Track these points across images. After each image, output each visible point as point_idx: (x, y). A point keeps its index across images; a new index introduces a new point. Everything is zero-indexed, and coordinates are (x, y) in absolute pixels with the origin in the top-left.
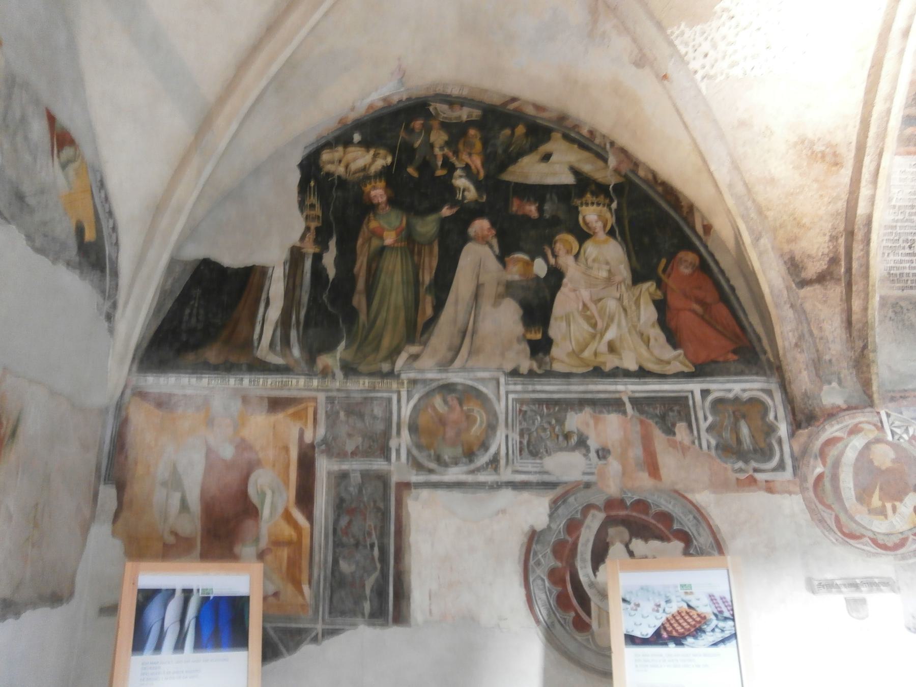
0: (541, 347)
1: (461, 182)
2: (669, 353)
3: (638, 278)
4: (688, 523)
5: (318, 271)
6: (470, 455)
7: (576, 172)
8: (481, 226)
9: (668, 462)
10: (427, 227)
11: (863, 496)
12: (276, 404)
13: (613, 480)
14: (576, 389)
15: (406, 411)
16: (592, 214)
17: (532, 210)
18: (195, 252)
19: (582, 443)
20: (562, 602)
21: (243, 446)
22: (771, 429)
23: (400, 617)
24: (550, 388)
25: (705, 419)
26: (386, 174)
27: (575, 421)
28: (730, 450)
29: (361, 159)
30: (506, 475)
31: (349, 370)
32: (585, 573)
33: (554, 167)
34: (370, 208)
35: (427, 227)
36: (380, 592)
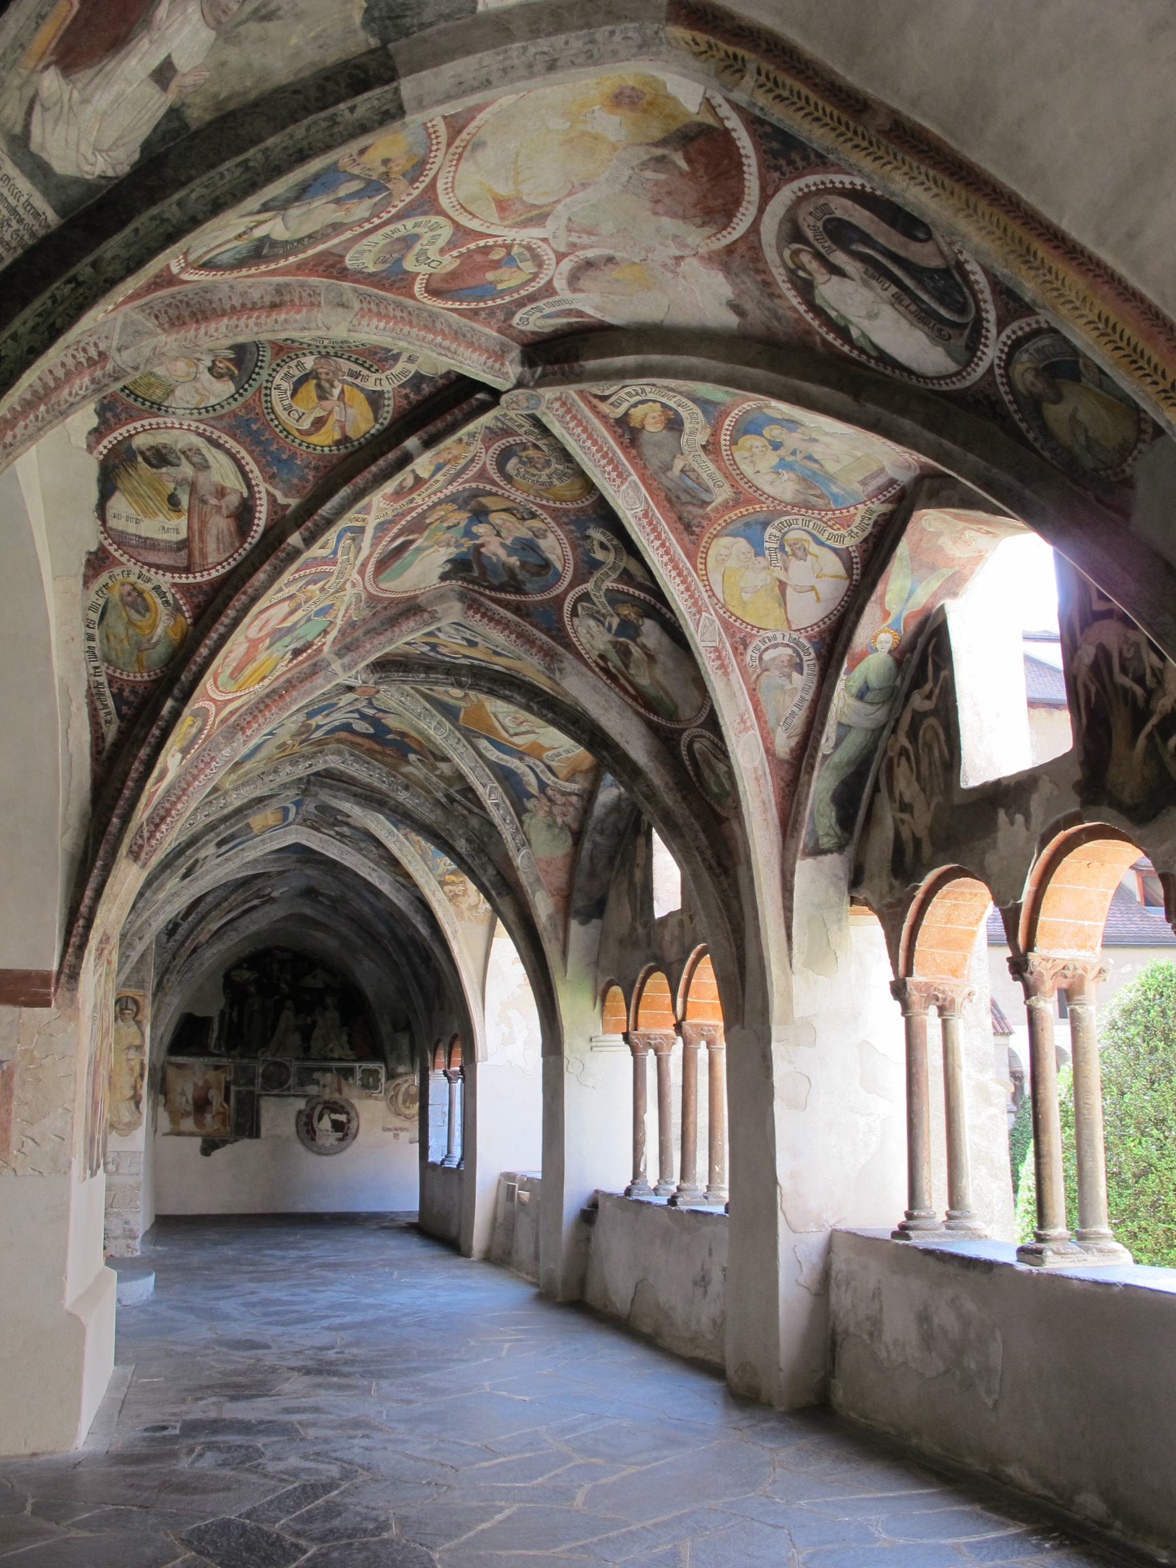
0: (307, 1049)
1: (283, 986)
8: (289, 1003)
9: (345, 1089)
11: (404, 1102)
12: (217, 1068)
13: (327, 1095)
16: (329, 1000)
18: (188, 1010)
21: (206, 1082)
23: (258, 1136)
24: (308, 1064)
25: (358, 1075)
27: (316, 1075)
28: (366, 1086)
29: (246, 975)
31: (242, 1056)
33: (317, 981)
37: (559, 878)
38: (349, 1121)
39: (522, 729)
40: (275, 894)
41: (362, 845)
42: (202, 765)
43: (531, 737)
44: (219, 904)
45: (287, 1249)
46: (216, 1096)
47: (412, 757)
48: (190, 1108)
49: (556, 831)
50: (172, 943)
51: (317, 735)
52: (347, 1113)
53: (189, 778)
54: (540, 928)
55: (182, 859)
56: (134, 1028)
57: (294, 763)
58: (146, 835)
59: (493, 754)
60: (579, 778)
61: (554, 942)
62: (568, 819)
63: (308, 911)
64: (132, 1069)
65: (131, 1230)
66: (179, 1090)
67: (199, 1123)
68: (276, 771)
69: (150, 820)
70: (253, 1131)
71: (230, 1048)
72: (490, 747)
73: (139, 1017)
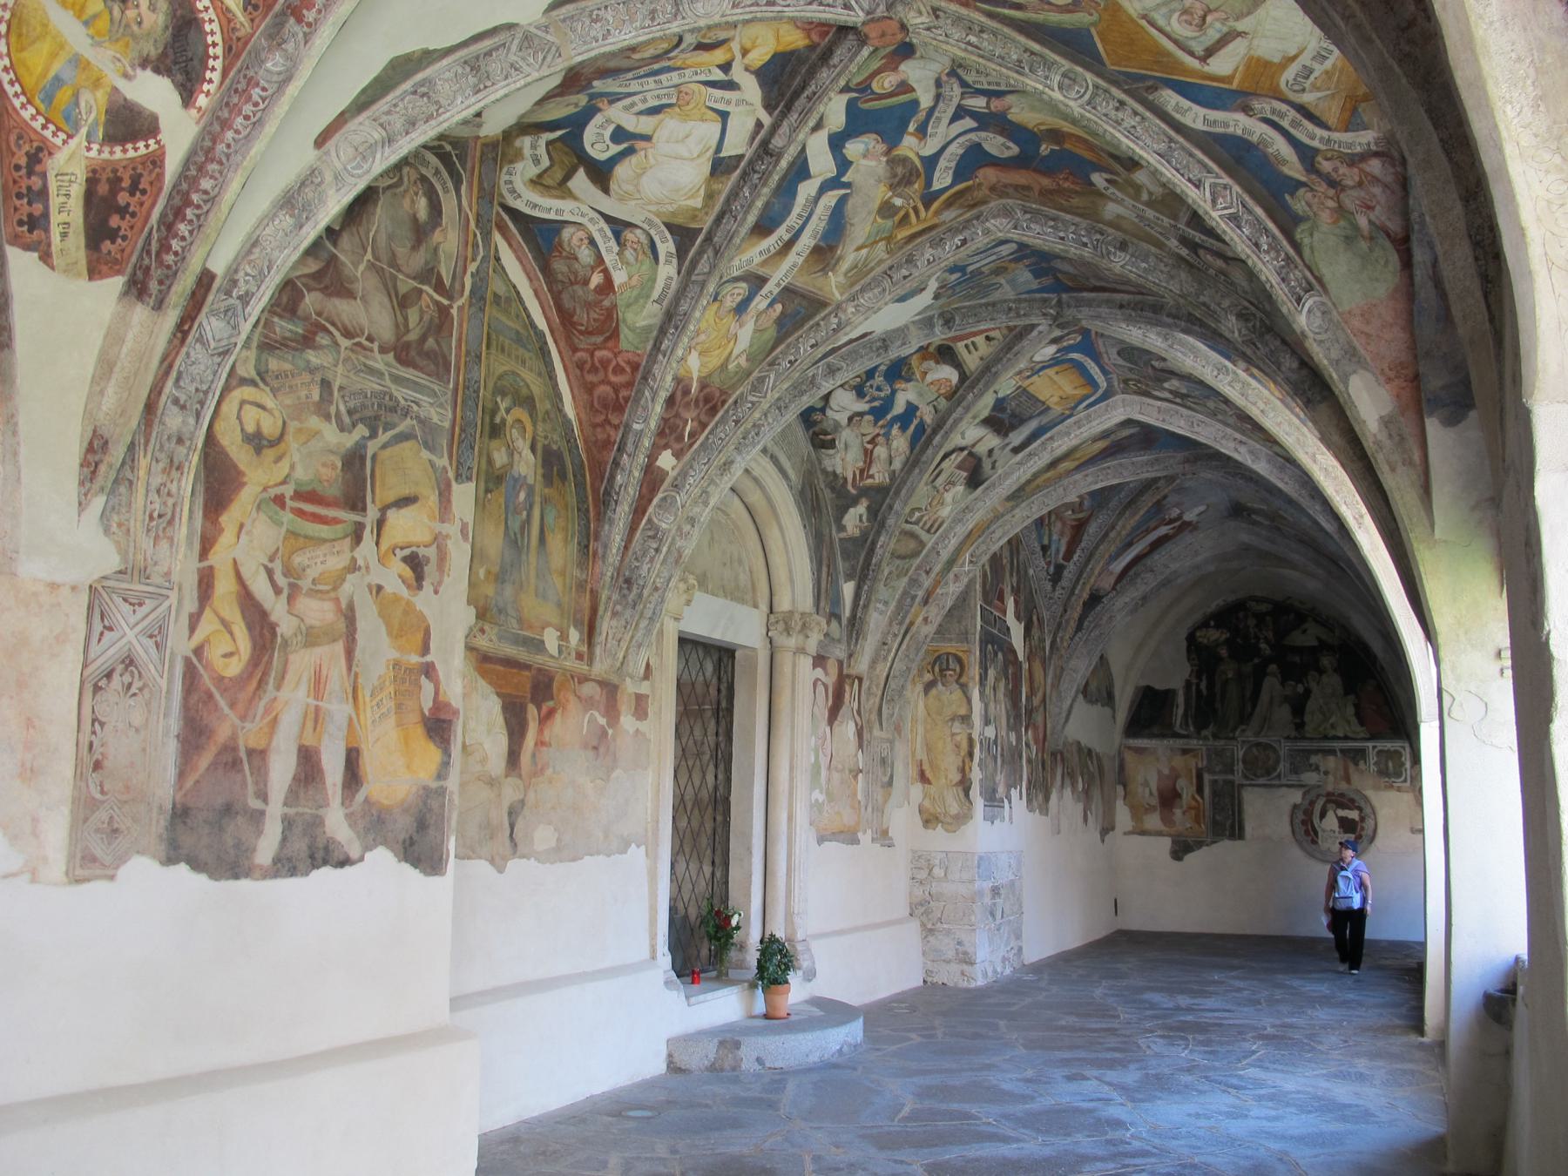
0: (1300, 726)
1: (1263, 645)
2: (1359, 729)
3: (1346, 694)
4: (1362, 804)
5: (1199, 691)
6: (1268, 773)
7: (1318, 639)
8: (1273, 667)
9: (1355, 777)
10: (1248, 668)
12: (1185, 752)
14: (1315, 745)
15: (1241, 754)
16: (1326, 661)
17: (1297, 659)
18: (1143, 683)
19: (1317, 769)
20: (1307, 833)
22: (1403, 764)
23: (1241, 836)
26: (1227, 640)
27: (1314, 759)
28: (1383, 772)
29: (1214, 635)
30: (1284, 781)
31: (1215, 737)
32: (1316, 821)
33: (1306, 637)
34: (1221, 659)
35: (1248, 668)
36: (1233, 827)
37: (1391, 344)
38: (1362, 819)
39: (1213, 35)
40: (1188, 517)
41: (1211, 404)
42: (235, 100)
43: (1237, 49)
44: (1106, 535)
45: (1203, 994)
46: (1186, 788)
47: (1098, 179)
48: (1155, 801)
49: (1364, 245)
50: (1059, 591)
51: (942, 179)
52: (1360, 809)
53: (217, 127)
54: (1369, 445)
55: (930, 451)
56: (958, 694)
57: (938, 243)
58: (154, 246)
59: (1196, 116)
60: (1367, 112)
61: (1400, 469)
62: (1379, 214)
63: (1244, 537)
64: (958, 746)
65: (965, 953)
66: (1140, 779)
67: (1168, 820)
68: (910, 260)
69: (161, 221)
70: (1237, 832)
71: (1200, 727)
72: (1185, 103)
73: (963, 680)
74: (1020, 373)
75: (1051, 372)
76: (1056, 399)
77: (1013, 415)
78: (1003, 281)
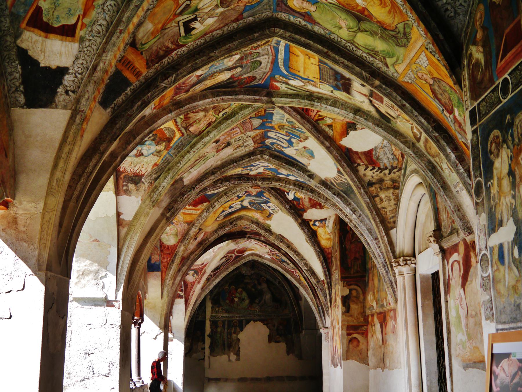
74: (315, 86)
75: (301, 74)
76: (312, 60)
77: (336, 79)
78: (285, 121)
